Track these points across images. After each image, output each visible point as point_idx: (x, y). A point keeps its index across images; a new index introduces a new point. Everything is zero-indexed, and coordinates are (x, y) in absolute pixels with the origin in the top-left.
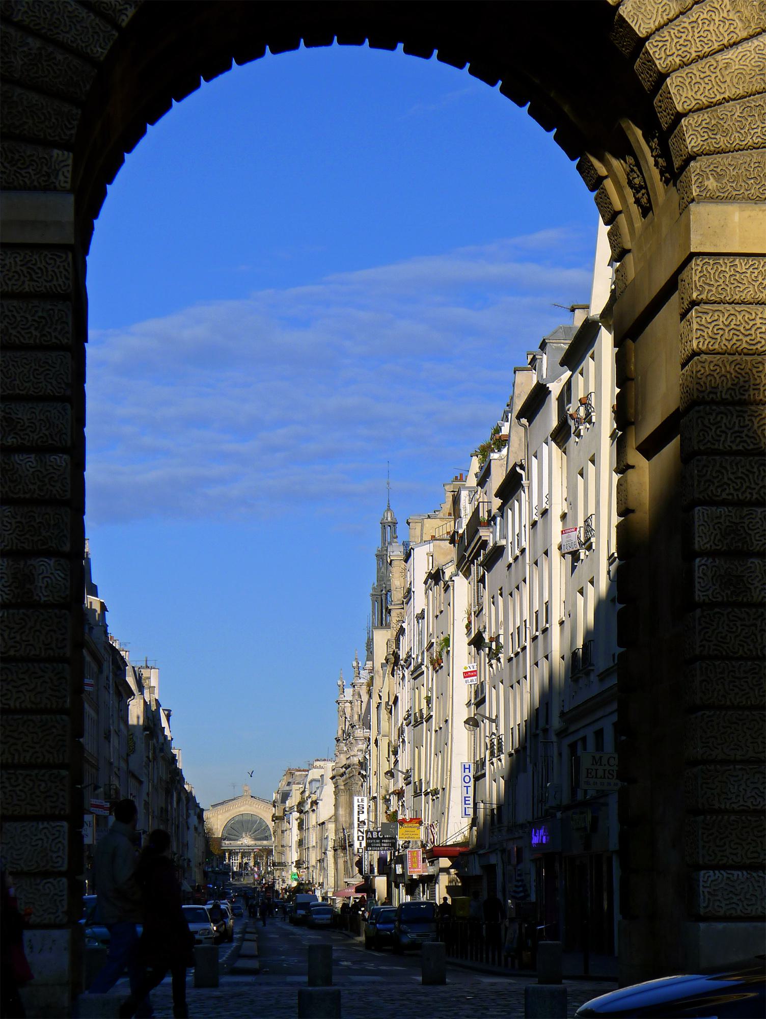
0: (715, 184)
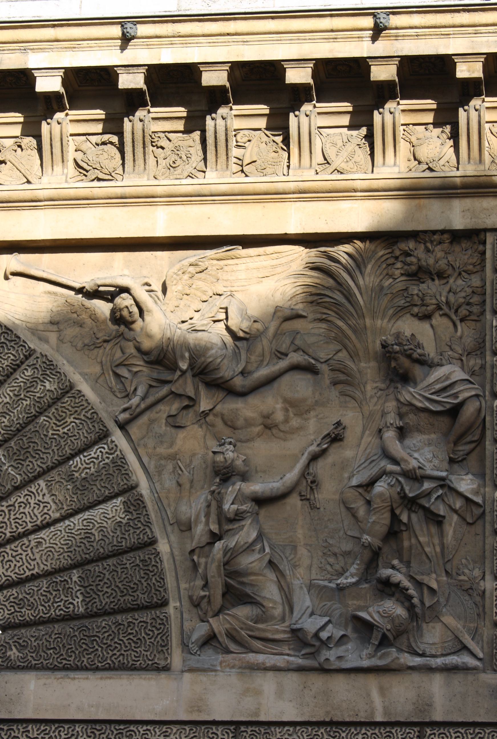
0: (17, 654)
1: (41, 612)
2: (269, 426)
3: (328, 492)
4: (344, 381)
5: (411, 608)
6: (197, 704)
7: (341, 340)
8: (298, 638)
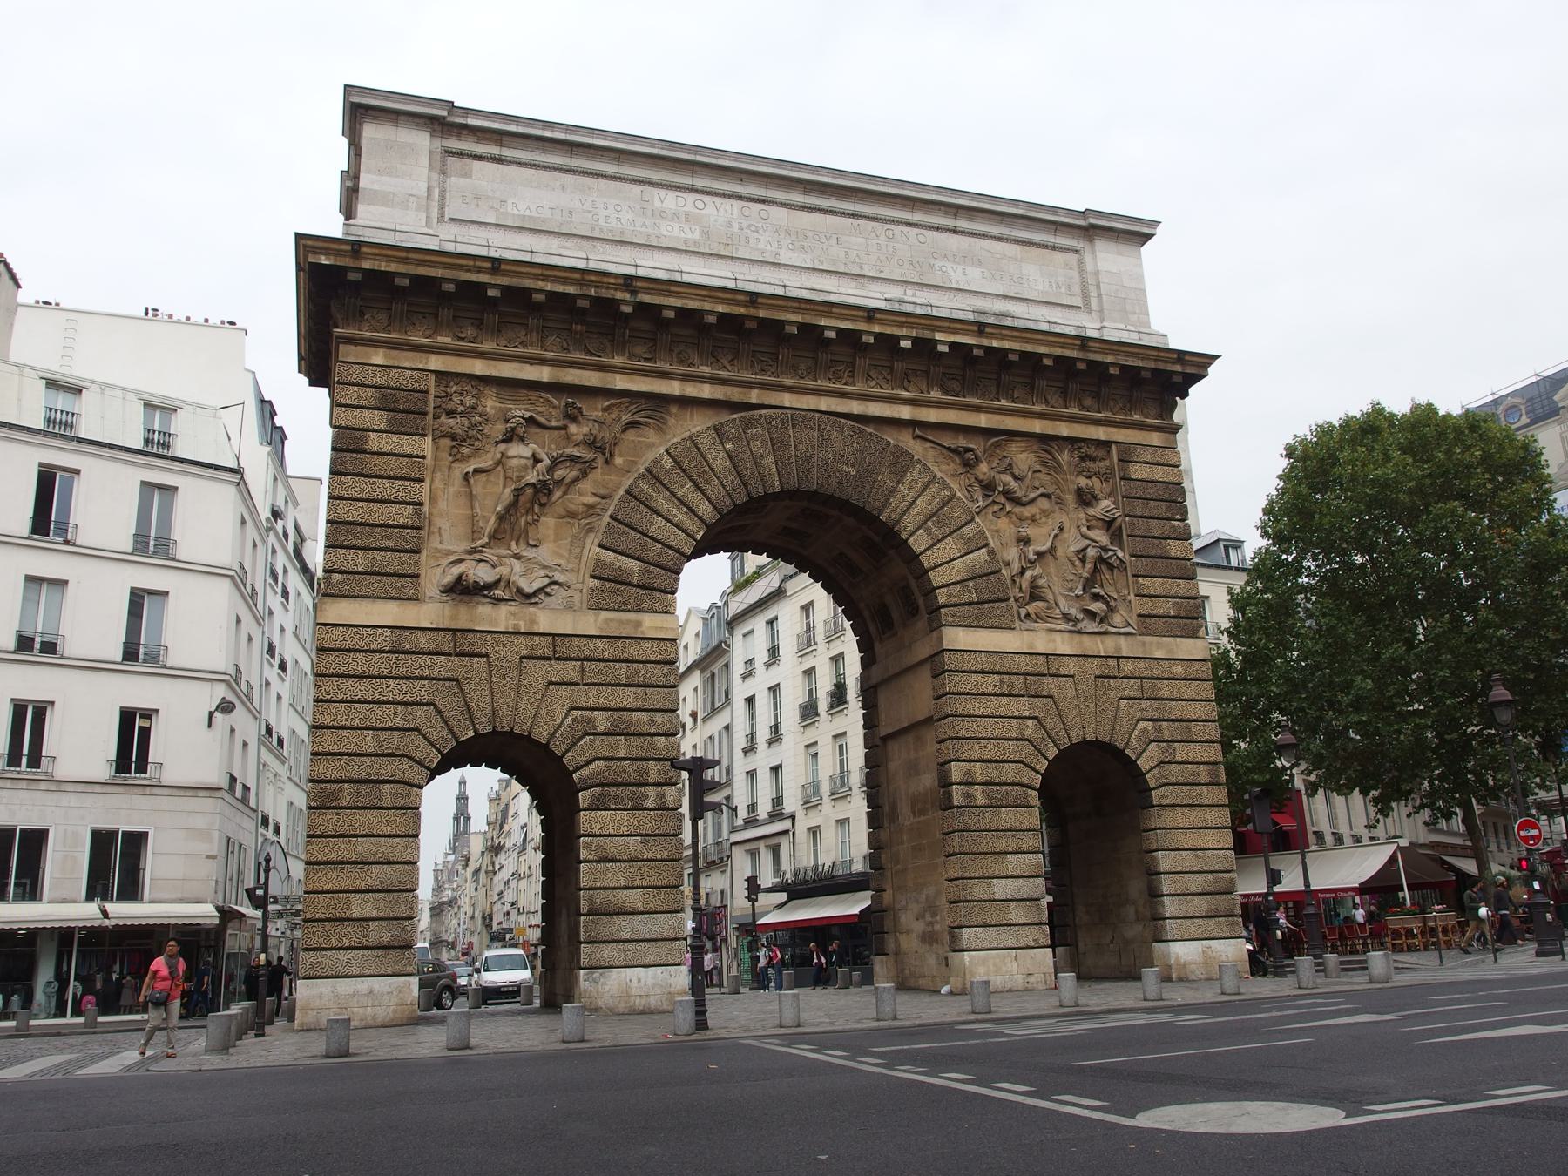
1: (958, 600)
2: (1033, 519)
3: (1060, 552)
4: (1060, 502)
5: (1108, 606)
6: (1031, 646)
7: (1057, 483)
8: (1067, 617)
